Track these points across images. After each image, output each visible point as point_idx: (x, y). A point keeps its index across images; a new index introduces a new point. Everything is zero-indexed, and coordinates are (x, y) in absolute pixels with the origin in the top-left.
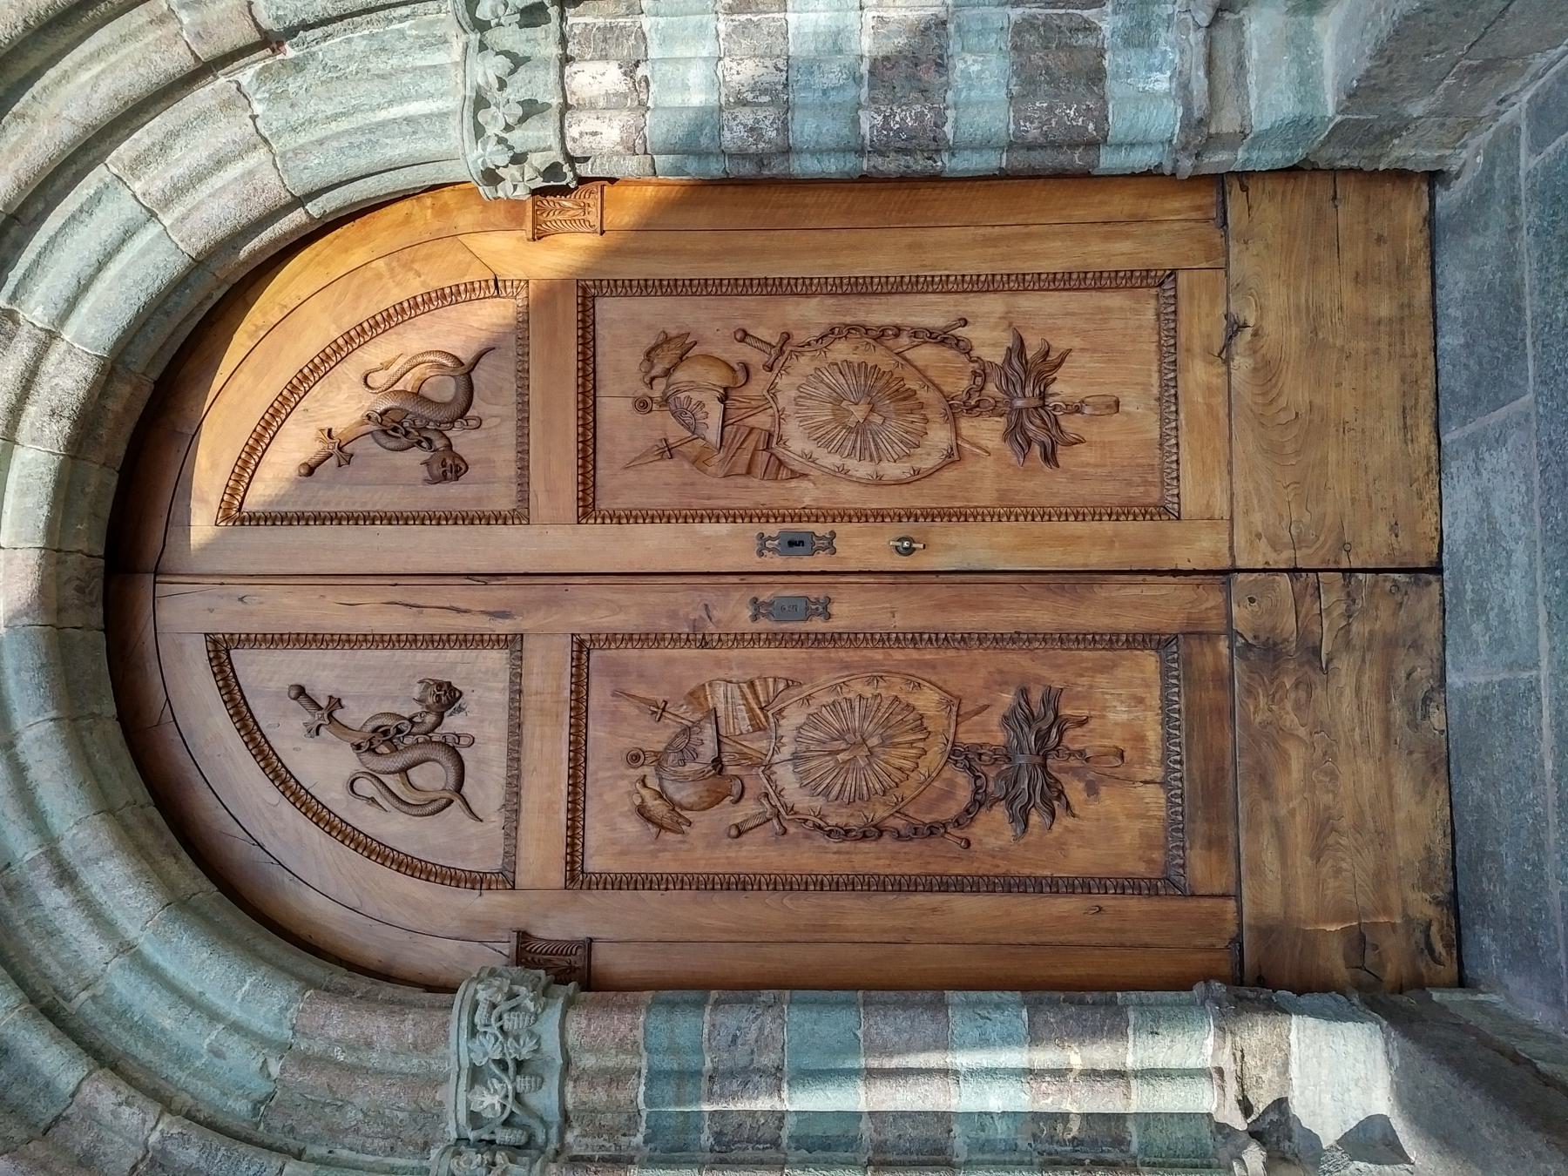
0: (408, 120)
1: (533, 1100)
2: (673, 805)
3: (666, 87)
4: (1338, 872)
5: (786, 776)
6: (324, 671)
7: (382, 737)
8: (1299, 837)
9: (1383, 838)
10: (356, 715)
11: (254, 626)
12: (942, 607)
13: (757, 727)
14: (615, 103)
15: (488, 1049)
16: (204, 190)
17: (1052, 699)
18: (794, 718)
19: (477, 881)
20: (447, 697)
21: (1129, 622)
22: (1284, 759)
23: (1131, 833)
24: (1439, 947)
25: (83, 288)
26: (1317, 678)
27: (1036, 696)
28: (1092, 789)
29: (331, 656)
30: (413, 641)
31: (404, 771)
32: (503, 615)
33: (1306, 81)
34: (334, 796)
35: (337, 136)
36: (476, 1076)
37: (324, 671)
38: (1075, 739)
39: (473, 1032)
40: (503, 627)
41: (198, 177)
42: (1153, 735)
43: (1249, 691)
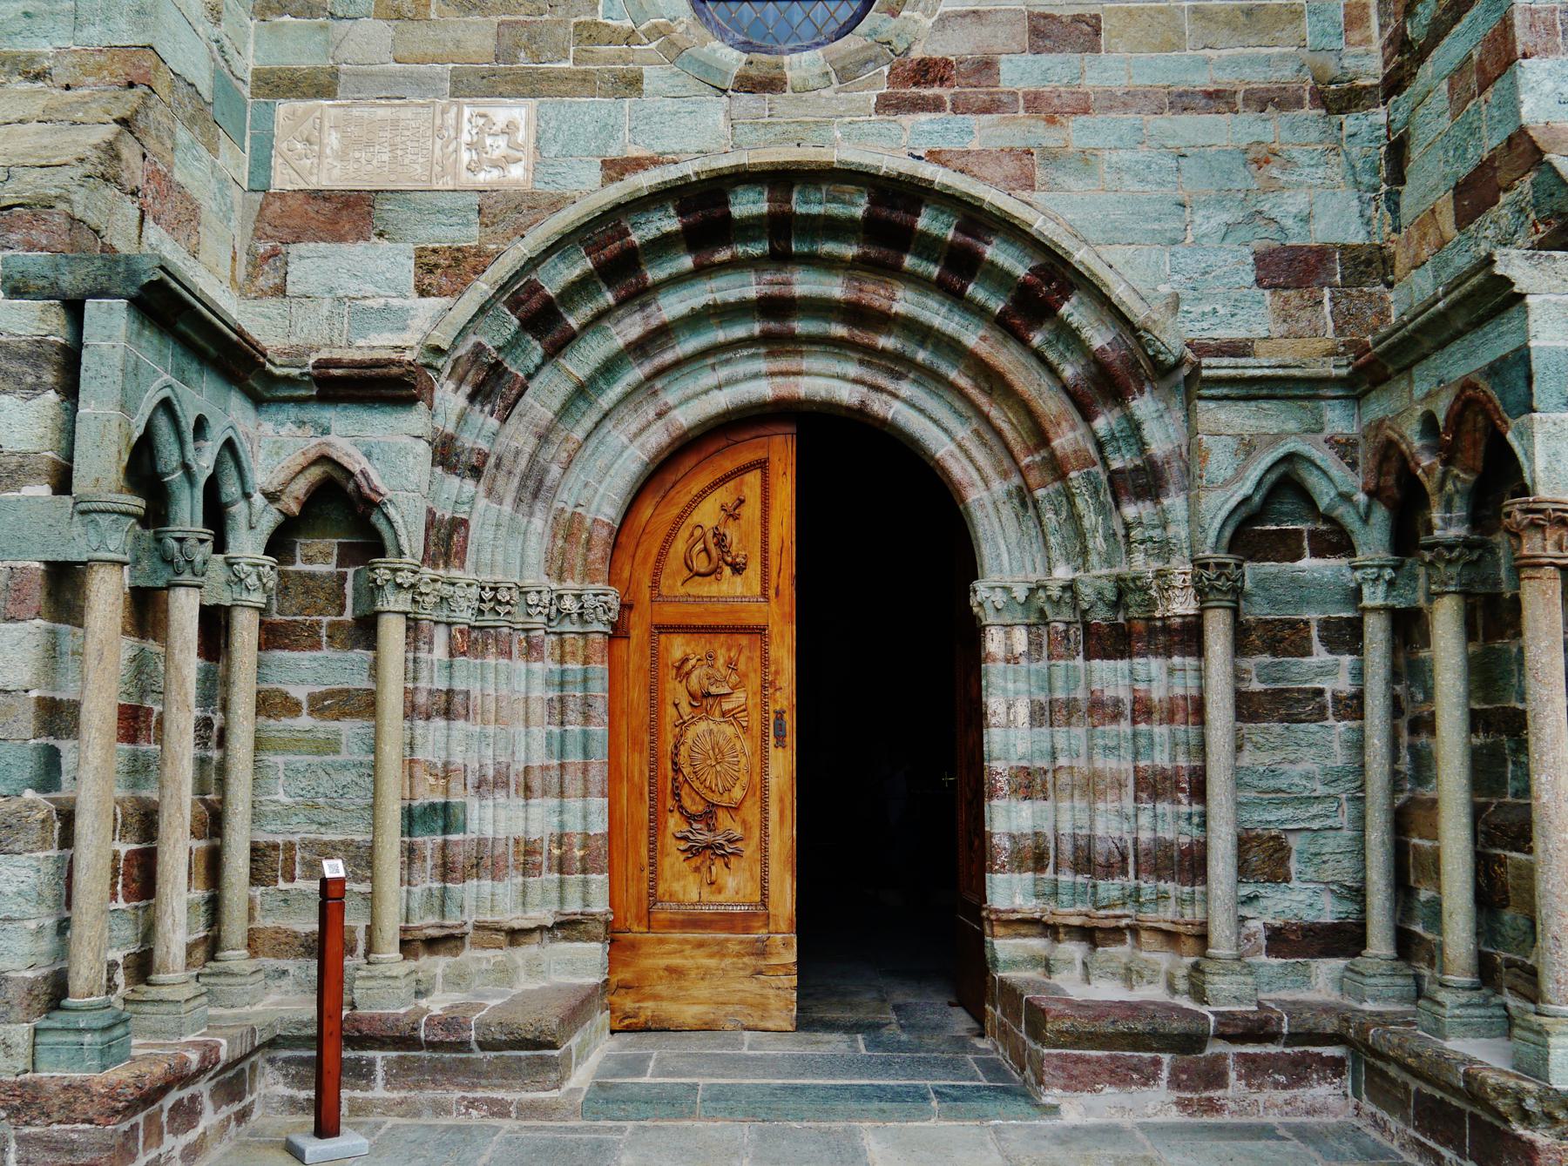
0: (998, 555)
1: (567, 620)
2: (688, 674)
3: (1015, 672)
4: (661, 978)
5: (702, 726)
6: (752, 510)
7: (720, 540)
8: (676, 961)
9: (674, 999)
10: (732, 533)
11: (772, 479)
12: (781, 800)
13: (723, 714)
14: (1009, 648)
15: (589, 600)
16: (965, 462)
17: (737, 854)
18: (729, 730)
19: (655, 585)
20: (738, 569)
21: (773, 887)
22: (711, 956)
23: (677, 887)
24: (627, 1022)
25: (921, 411)
26: (748, 972)
27: (739, 845)
28: (697, 869)
29: (758, 513)
30: (765, 550)
31: (705, 549)
32: (777, 594)
33: (1013, 964)
34: (696, 517)
35: (991, 524)
36: (578, 597)
37: (752, 510)
38: (719, 863)
39: (596, 595)
40: (772, 593)
41: (971, 460)
42: (721, 898)
43: (741, 942)
